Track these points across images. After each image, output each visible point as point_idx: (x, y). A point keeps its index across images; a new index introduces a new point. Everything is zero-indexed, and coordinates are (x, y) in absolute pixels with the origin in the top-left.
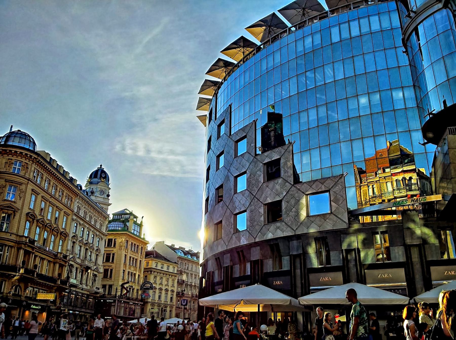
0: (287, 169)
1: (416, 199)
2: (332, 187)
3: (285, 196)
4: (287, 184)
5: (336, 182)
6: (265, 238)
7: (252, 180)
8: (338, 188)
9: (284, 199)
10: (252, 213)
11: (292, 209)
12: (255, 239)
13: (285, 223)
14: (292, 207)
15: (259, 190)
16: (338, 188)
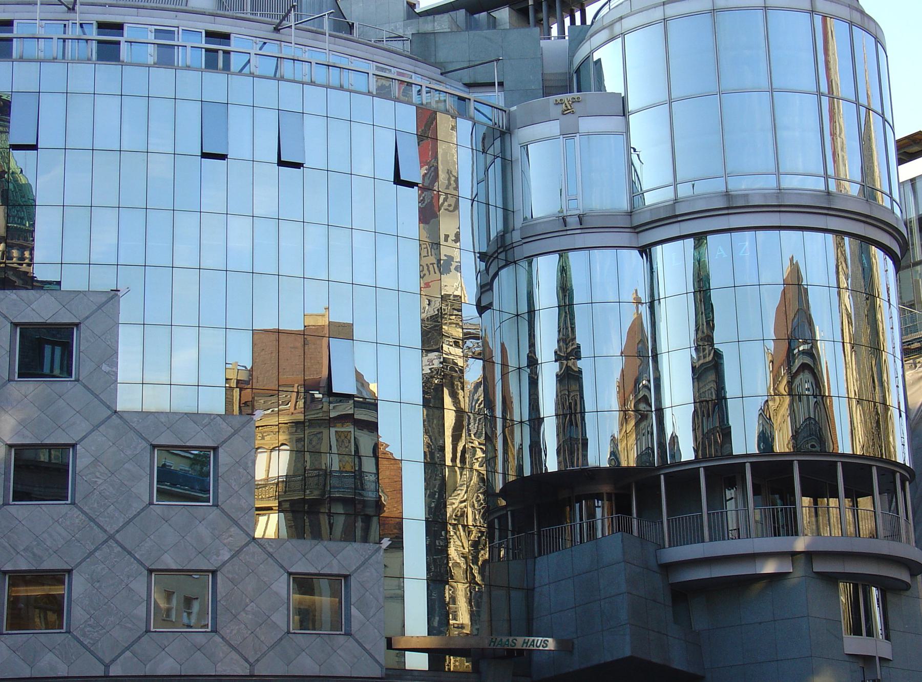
0: (236, 488)
1: (531, 641)
2: (356, 570)
3: (224, 564)
4: (234, 530)
5: (366, 560)
6: (148, 670)
7: (100, 481)
8: (368, 574)
9: (225, 569)
10: (100, 587)
11: (247, 606)
12: (107, 666)
13: (223, 638)
14: (248, 600)
15: (131, 520)
16: (368, 574)
